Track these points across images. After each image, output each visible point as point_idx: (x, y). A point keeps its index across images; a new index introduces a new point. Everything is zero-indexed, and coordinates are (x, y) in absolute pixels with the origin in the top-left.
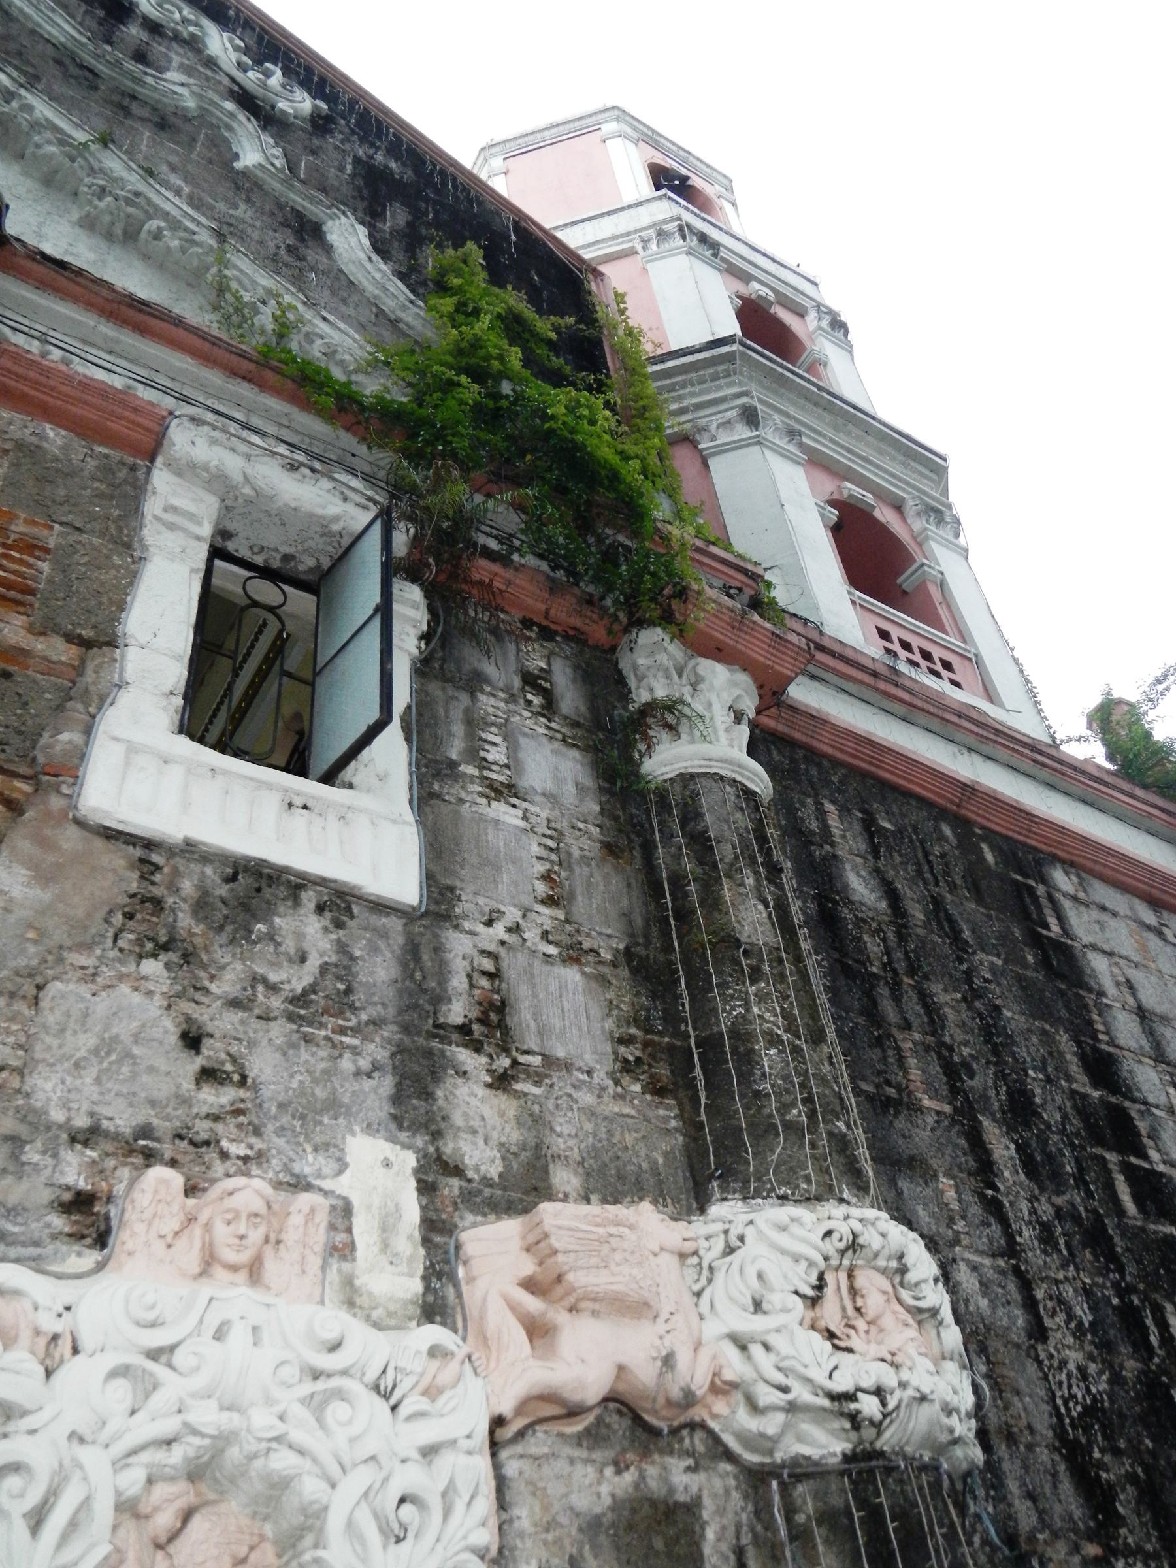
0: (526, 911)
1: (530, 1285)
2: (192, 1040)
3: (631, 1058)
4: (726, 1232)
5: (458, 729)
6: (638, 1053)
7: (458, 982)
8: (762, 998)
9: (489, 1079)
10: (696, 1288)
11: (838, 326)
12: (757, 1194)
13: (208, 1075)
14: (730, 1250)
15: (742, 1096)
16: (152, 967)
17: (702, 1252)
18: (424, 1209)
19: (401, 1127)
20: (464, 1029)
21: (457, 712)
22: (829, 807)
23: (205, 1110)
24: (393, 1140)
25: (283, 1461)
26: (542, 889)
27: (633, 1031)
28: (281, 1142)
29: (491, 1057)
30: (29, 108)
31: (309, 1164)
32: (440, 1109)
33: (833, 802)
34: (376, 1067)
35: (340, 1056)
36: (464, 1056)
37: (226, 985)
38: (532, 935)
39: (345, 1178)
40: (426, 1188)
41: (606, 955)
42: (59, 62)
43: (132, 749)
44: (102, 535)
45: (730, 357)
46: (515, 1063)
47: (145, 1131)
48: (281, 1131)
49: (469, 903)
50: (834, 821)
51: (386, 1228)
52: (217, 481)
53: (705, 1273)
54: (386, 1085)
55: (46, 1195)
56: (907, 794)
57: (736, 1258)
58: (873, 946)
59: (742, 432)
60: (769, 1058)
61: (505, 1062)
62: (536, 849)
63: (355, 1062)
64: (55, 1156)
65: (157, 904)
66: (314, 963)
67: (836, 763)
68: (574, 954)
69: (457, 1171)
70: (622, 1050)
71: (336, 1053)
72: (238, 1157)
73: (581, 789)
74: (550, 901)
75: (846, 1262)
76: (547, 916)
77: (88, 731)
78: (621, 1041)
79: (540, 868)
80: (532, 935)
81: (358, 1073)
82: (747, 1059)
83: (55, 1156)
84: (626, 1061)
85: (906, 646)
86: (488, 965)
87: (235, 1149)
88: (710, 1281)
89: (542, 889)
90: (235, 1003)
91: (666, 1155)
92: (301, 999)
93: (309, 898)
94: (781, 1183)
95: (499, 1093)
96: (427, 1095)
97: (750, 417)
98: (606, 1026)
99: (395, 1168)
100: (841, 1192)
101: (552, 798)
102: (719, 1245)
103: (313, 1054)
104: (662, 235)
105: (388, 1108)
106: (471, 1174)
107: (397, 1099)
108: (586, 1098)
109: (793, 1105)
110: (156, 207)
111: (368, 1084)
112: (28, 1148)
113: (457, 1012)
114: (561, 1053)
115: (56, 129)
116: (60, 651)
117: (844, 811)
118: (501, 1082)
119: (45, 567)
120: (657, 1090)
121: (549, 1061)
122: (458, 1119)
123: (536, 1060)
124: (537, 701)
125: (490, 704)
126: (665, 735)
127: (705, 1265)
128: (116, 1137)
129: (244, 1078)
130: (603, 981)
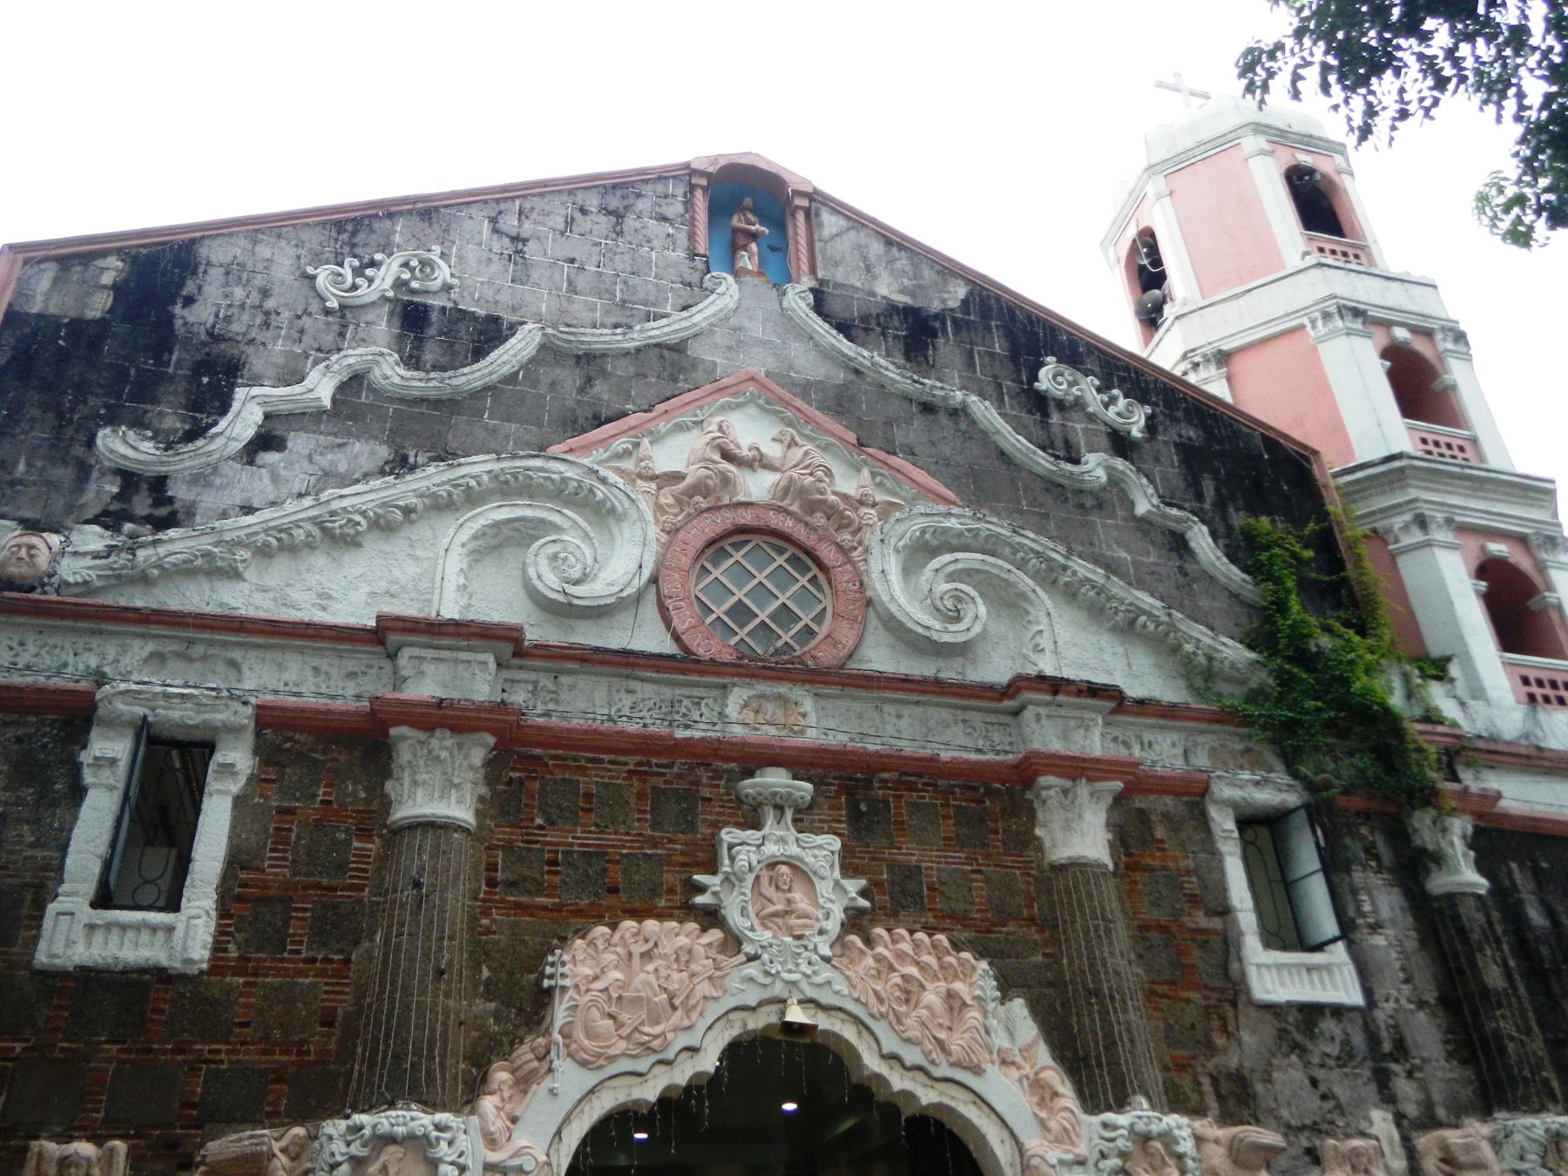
0: (1399, 990)
1: (1443, 1160)
2: (1314, 1083)
5: (1349, 898)
7: (1384, 1034)
8: (1504, 1017)
11: (1460, 337)
13: (1324, 1097)
14: (1507, 1136)
16: (1294, 1058)
20: (1391, 1054)
21: (1347, 890)
22: (1514, 865)
26: (1401, 975)
30: (1075, 573)
31: (1363, 1125)
33: (1515, 861)
36: (1394, 1067)
37: (1316, 1060)
38: (1403, 1002)
40: (1398, 1125)
41: (1432, 1001)
42: (1048, 490)
43: (1258, 966)
44: (1205, 851)
45: (1401, 470)
47: (1315, 1123)
49: (1379, 994)
50: (1517, 876)
51: (1391, 1143)
52: (1234, 805)
54: (1373, 1087)
56: (1553, 837)
58: (1545, 951)
59: (1416, 536)
60: (1511, 1046)
61: (1408, 1066)
62: (1394, 955)
65: (1285, 1031)
66: (1338, 1040)
67: (1514, 833)
68: (1421, 1004)
73: (1402, 909)
74: (1406, 981)
76: (1406, 989)
77: (1240, 959)
79: (1398, 965)
80: (1403, 1002)
82: (1502, 1049)
85: (1540, 683)
86: (1391, 1022)
89: (1401, 975)
90: (1322, 1066)
92: (1338, 1059)
93: (1327, 1012)
96: (1387, 1087)
97: (1422, 522)
101: (1393, 922)
104: (1327, 316)
107: (1380, 1092)
108: (1440, 1074)
110: (1139, 608)
113: (1387, 1047)
114: (1425, 1054)
115: (1088, 580)
116: (1216, 923)
117: (1521, 865)
118: (1410, 1074)
119: (1194, 879)
120: (1464, 1062)
121: (1424, 1060)
124: (1373, 864)
125: (1358, 876)
126: (1433, 866)
130: (1434, 1015)
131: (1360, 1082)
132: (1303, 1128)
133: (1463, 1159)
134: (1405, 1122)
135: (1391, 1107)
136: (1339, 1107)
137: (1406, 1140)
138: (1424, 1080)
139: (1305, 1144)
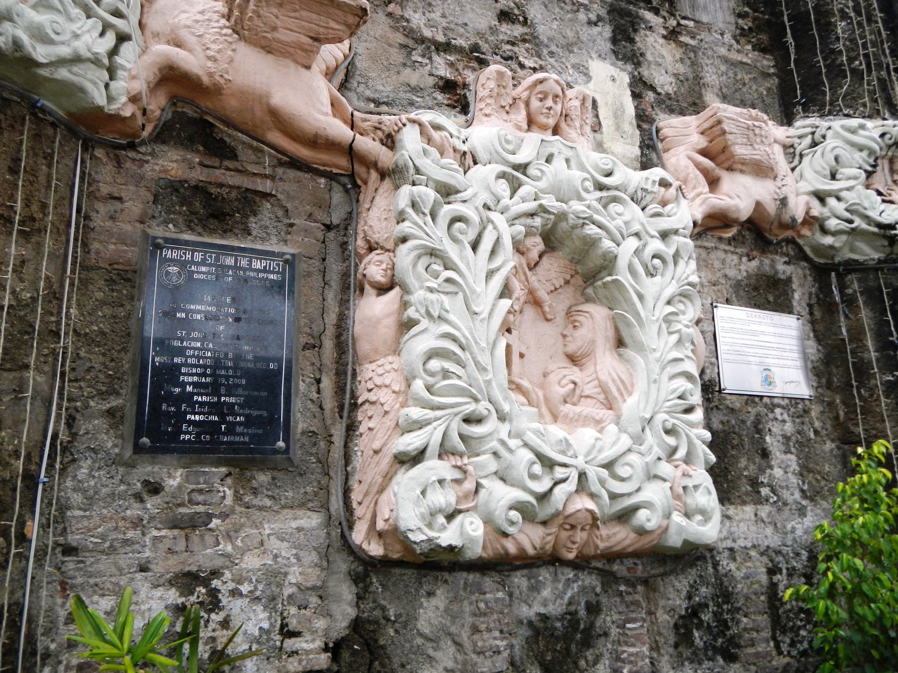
1: (704, 153)
3: (746, 27)
4: (813, 133)
6: (750, 24)
9: (665, 33)
10: (793, 165)
12: (830, 113)
14: (814, 144)
15: (822, 52)
17: (796, 145)
18: (636, 107)
19: (617, 59)
23: (506, 38)
24: (613, 64)
25: (591, 230)
27: (746, 9)
28: (552, 60)
29: (664, 18)
32: (639, 49)
34: (600, 19)
35: (578, 11)
39: (591, 85)
40: (636, 96)
46: (679, 24)
47: (475, 48)
48: (552, 54)
51: (618, 115)
53: (797, 158)
54: (607, 31)
55: (431, 81)
57: (819, 149)
60: (841, 26)
61: (673, 22)
63: (587, 14)
64: (430, 58)
69: (652, 88)
70: (740, 21)
71: (575, 8)
72: (530, 68)
75: (890, 154)
78: (740, 15)
81: (590, 23)
82: (827, 28)
83: (430, 58)
84: (743, 29)
87: (529, 63)
88: (800, 162)
91: (769, 90)
94: (847, 106)
95: (671, 42)
98: (731, 5)
99: (618, 82)
100: (884, 114)
102: (808, 140)
103: (562, 8)
105: (609, 45)
106: (659, 90)
107: (614, 41)
109: (856, 58)
111: (596, 30)
112: (414, 53)
114: (705, 19)
118: (672, 35)
122: (649, 57)
123: (691, 24)
127: (798, 152)
128: (459, 50)
129: (526, 19)
131: (582, 16)
132: (445, 47)
133: (741, 151)
134: (650, 96)
135: (629, 67)
136: (531, 39)
137: (643, 118)
138: (694, 50)
139: (444, 72)
